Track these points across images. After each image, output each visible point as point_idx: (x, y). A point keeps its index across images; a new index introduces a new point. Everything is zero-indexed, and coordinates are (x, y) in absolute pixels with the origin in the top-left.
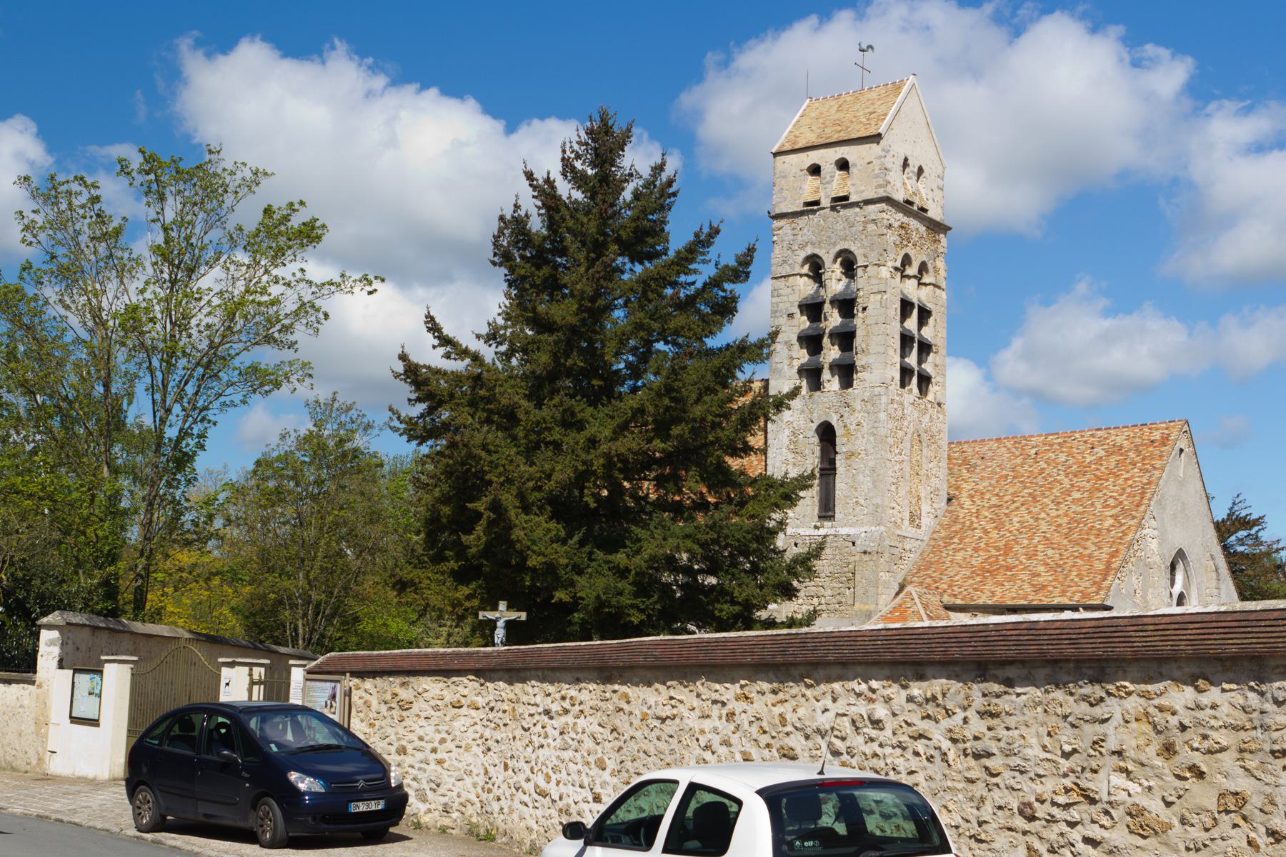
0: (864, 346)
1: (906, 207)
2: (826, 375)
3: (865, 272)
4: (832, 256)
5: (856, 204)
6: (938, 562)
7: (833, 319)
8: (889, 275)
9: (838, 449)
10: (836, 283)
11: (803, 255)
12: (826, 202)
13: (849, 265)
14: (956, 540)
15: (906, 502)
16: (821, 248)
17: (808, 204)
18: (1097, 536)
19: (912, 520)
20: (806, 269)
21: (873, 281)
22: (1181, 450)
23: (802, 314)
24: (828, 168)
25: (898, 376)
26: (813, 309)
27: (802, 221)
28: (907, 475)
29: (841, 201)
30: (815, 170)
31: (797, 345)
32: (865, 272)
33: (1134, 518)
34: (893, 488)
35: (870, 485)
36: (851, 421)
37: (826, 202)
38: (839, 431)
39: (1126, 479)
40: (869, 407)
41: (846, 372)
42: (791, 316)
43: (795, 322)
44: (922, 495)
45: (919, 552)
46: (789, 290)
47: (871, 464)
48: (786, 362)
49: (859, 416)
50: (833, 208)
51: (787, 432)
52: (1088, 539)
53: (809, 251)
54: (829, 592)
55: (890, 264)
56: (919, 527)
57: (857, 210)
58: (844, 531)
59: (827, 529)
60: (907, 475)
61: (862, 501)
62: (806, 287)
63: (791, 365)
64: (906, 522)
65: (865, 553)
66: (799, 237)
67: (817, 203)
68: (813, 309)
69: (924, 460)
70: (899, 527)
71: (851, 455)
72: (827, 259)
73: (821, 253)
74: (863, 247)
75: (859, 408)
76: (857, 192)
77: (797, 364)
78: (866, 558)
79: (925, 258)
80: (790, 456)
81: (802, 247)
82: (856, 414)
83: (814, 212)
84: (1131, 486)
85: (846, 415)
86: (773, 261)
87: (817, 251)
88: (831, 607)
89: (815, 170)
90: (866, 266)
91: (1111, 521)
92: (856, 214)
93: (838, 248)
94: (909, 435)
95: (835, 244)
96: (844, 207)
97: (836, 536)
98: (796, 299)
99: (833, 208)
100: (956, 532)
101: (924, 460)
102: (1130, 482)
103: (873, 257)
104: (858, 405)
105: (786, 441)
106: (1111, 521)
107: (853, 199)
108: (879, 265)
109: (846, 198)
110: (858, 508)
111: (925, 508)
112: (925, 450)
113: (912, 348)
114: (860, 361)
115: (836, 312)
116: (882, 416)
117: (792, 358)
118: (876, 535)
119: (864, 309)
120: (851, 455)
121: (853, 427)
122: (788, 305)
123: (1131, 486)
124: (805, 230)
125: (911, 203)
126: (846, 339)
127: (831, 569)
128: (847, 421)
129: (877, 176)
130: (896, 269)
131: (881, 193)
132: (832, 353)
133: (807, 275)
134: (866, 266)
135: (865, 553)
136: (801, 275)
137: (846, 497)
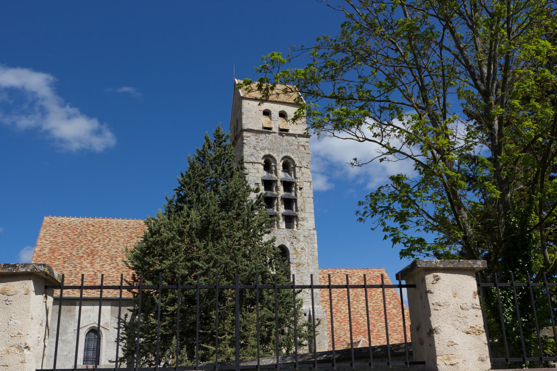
0: (302, 208)
3: (300, 170)
4: (280, 158)
11: (263, 154)
13: (288, 165)
16: (274, 153)
20: (262, 161)
24: (275, 114)
27: (262, 136)
29: (283, 132)
30: (267, 113)
36: (298, 246)
38: (291, 251)
40: (308, 240)
46: (256, 171)
49: (302, 244)
53: (267, 152)
57: (294, 138)
71: (299, 265)
81: (263, 149)
82: (301, 243)
85: (294, 243)
90: (301, 167)
92: (294, 140)
93: (284, 155)
99: (280, 134)
104: (301, 238)
107: (291, 132)
109: (287, 130)
119: (301, 189)
120: (299, 265)
121: (299, 250)
122: (255, 178)
124: (264, 141)
126: (289, 203)
128: (296, 247)
134: (301, 167)
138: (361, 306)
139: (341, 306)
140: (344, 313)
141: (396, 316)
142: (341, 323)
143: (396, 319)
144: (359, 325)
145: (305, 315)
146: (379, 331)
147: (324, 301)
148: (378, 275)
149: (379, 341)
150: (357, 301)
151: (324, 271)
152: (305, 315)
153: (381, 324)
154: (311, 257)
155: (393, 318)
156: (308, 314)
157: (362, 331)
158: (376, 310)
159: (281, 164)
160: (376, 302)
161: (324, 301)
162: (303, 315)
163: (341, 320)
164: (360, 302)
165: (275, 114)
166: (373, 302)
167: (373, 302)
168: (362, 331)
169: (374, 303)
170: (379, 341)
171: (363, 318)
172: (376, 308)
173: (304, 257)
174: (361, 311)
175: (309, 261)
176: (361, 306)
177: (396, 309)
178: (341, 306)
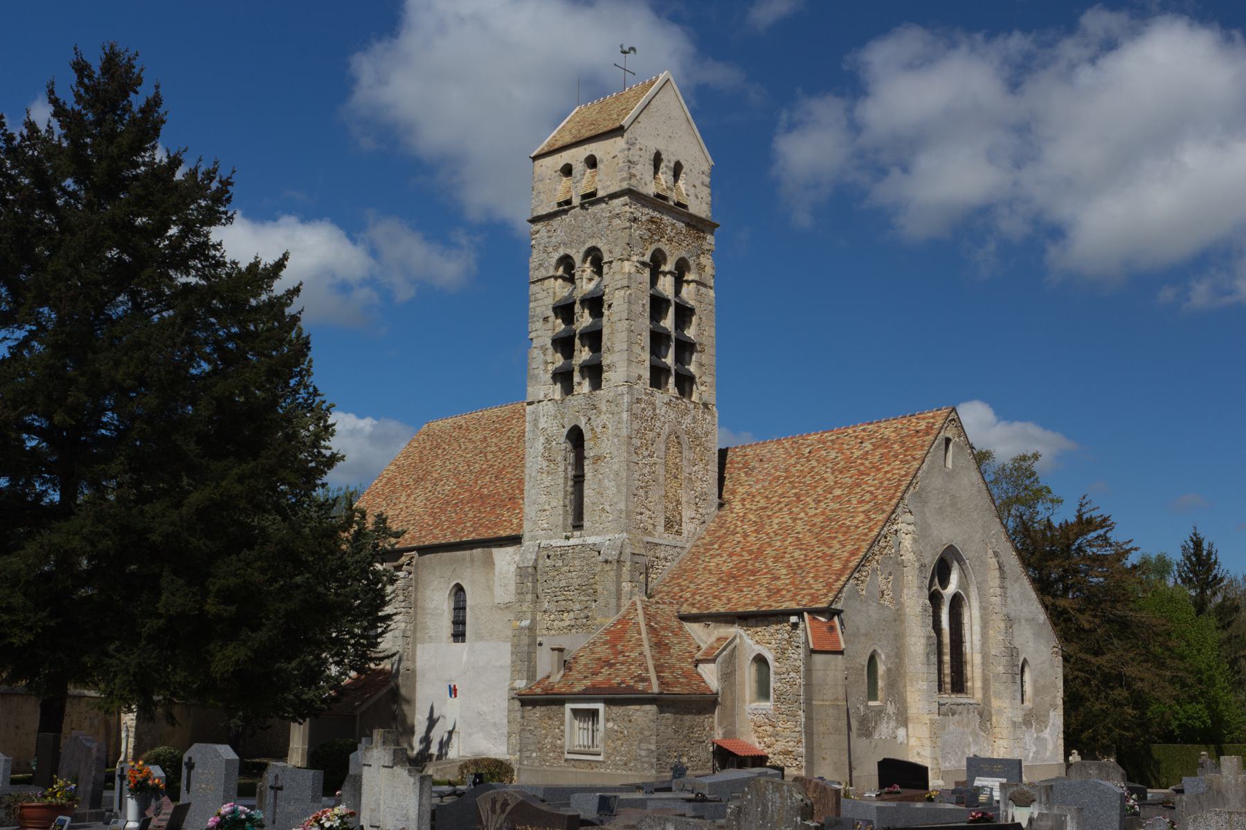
0: (609, 344)
1: (658, 201)
2: (577, 378)
4: (581, 255)
5: (601, 200)
6: (692, 570)
7: (584, 320)
8: (633, 270)
9: (586, 454)
10: (586, 285)
12: (576, 201)
14: (716, 546)
15: (660, 507)
16: (572, 248)
17: (560, 204)
18: (845, 533)
19: (669, 525)
20: (561, 271)
21: (617, 277)
22: (948, 441)
23: (557, 317)
24: (579, 167)
25: (647, 375)
26: (565, 311)
28: (661, 479)
29: (590, 198)
31: (551, 350)
32: (610, 268)
33: (884, 511)
34: (641, 492)
37: (576, 201)
38: (587, 435)
39: (887, 472)
41: (594, 372)
42: (546, 319)
43: (550, 325)
44: (684, 500)
45: (677, 560)
47: (615, 467)
48: (542, 367)
50: (582, 206)
51: (542, 440)
52: (835, 538)
53: (562, 252)
54: (578, 606)
55: (635, 258)
56: (679, 533)
57: (604, 205)
58: (590, 540)
60: (661, 479)
61: (607, 508)
62: (560, 290)
63: (546, 370)
64: (661, 529)
65: (606, 562)
66: (554, 240)
67: (568, 202)
68: (565, 311)
69: (685, 462)
70: (650, 534)
71: (598, 459)
72: (578, 259)
73: (572, 252)
74: (609, 243)
75: (604, 409)
76: (603, 188)
77: (551, 368)
78: (607, 567)
79: (684, 254)
80: (545, 464)
81: (556, 248)
83: (565, 212)
84: (889, 480)
85: (593, 417)
86: (531, 266)
87: (568, 251)
88: (579, 622)
89: (567, 170)
90: (611, 262)
91: (861, 517)
93: (588, 245)
94: (663, 437)
95: (584, 243)
96: (592, 204)
97: (583, 546)
98: (550, 302)
99: (582, 206)
100: (719, 537)
101: (685, 462)
102: (889, 475)
103: (618, 252)
104: (603, 407)
105: (541, 448)
106: (861, 517)
107: (600, 194)
108: (622, 260)
109: (593, 194)
111: (687, 513)
112: (685, 453)
113: (668, 347)
114: (606, 360)
115: (587, 312)
116: (625, 415)
117: (546, 363)
118: (619, 542)
119: (610, 306)
120: (598, 459)
121: (599, 430)
123: (889, 480)
125: (665, 198)
126: (594, 338)
127: (579, 581)
128: (594, 424)
129: (621, 170)
130: (644, 264)
131: (625, 185)
132: (583, 355)
133: (561, 277)
134: (611, 262)
136: (556, 278)
137: (594, 504)
159: (588, 264)
165: (579, 167)
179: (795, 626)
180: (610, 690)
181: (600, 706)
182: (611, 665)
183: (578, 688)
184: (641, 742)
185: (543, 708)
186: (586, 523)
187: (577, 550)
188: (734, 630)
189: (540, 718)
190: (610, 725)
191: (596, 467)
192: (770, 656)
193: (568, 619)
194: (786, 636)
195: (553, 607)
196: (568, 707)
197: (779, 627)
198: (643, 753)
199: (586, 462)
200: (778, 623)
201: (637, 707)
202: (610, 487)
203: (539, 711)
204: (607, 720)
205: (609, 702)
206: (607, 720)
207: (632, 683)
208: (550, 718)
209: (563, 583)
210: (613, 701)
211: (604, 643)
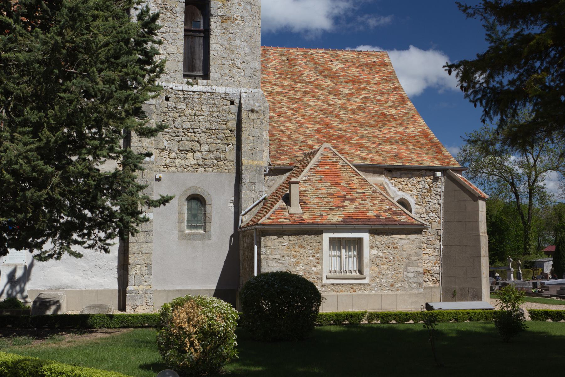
35: (248, 51)
47: (248, 30)
58: (221, 90)
59: (201, 86)
65: (252, 111)
88: (207, 162)
97: (212, 93)
110: (235, 70)
120: (226, 19)
127: (208, 125)
135: (252, 111)
137: (222, 58)
138: (340, 102)
139: (309, 100)
140: (311, 110)
141: (395, 119)
142: (302, 124)
143: (393, 123)
144: (332, 128)
145: (232, 103)
146: (362, 138)
147: (282, 92)
148: (375, 60)
149: (359, 153)
150: (335, 95)
151: (291, 51)
152: (232, 103)
153: (367, 128)
154: (249, 7)
155: (390, 122)
156: (237, 101)
157: (334, 137)
158: (364, 108)
160: (365, 97)
161: (282, 92)
162: (229, 103)
163: (303, 121)
164: (341, 97)
166: (361, 97)
167: (361, 97)
168: (334, 137)
169: (362, 99)
170: (359, 153)
171: (340, 118)
172: (364, 105)
173: (237, 6)
174: (339, 109)
175: (245, 14)
176: (340, 102)
177: (396, 108)
178: (309, 100)
179: (436, 179)
180: (368, 221)
181: (366, 236)
182: (353, 200)
183: (335, 217)
184: (407, 265)
185: (292, 238)
186: (212, 74)
187: (204, 96)
188: (382, 179)
189: (289, 247)
190: (374, 252)
191: (224, 25)
192: (412, 201)
193: (191, 159)
194: (427, 187)
195: (175, 146)
196: (326, 237)
197: (421, 179)
198: (411, 275)
199: (213, 20)
200: (420, 176)
201: (403, 236)
202: (242, 46)
203: (286, 240)
204: (372, 248)
205: (373, 232)
206: (372, 248)
207: (388, 215)
208: (302, 247)
209: (187, 125)
210: (381, 229)
211: (322, 180)
